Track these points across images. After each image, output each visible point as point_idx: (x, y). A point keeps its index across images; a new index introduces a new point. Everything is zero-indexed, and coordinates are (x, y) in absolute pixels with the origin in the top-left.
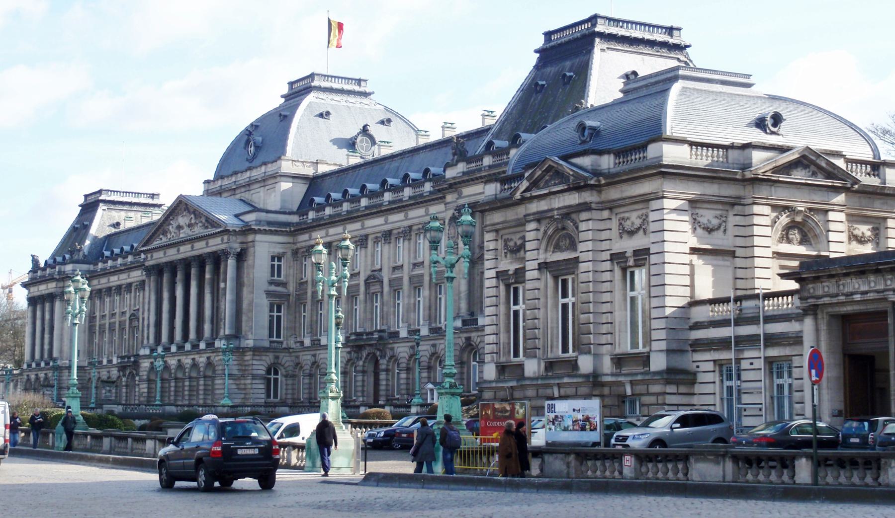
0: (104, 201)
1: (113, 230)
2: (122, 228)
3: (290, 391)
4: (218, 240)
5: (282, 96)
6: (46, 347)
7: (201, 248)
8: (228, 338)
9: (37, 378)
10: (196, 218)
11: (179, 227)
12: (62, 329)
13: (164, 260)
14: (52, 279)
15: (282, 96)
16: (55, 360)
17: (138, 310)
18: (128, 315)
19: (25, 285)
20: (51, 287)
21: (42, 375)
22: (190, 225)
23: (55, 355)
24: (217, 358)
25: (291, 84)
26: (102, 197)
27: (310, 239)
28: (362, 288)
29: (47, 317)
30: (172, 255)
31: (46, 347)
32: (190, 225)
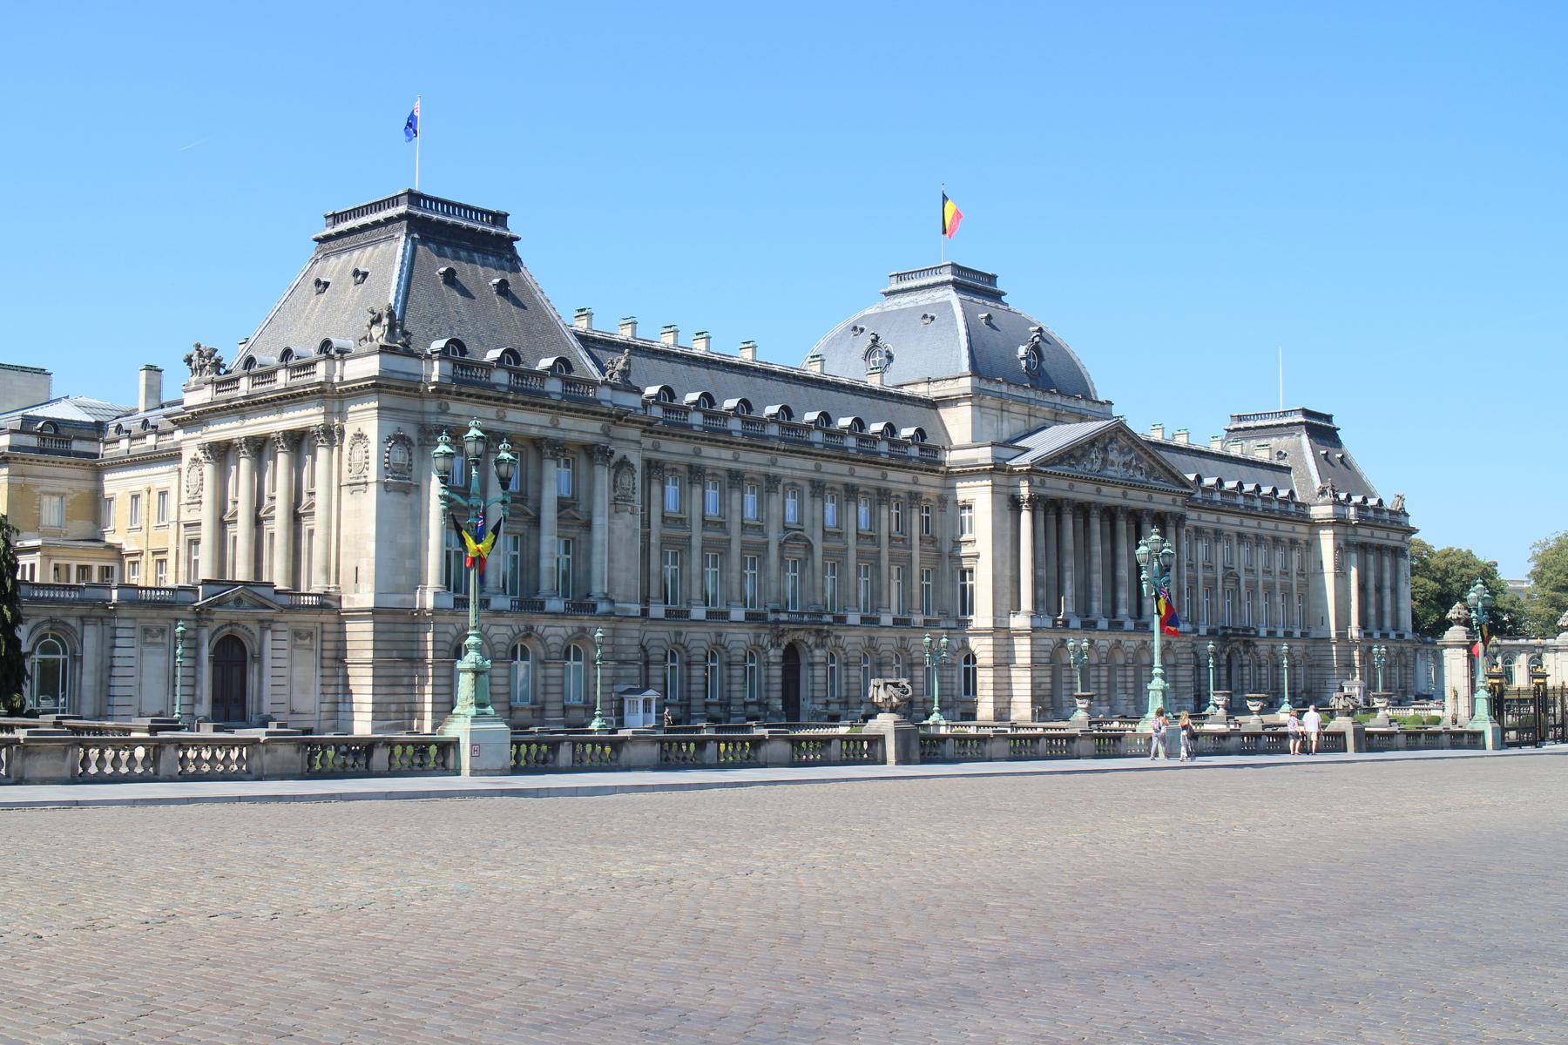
4: (1169, 499)
7: (1137, 499)
13: (1070, 495)
22: (1127, 465)
28: (1220, 583)
30: (1085, 492)
32: (1127, 465)
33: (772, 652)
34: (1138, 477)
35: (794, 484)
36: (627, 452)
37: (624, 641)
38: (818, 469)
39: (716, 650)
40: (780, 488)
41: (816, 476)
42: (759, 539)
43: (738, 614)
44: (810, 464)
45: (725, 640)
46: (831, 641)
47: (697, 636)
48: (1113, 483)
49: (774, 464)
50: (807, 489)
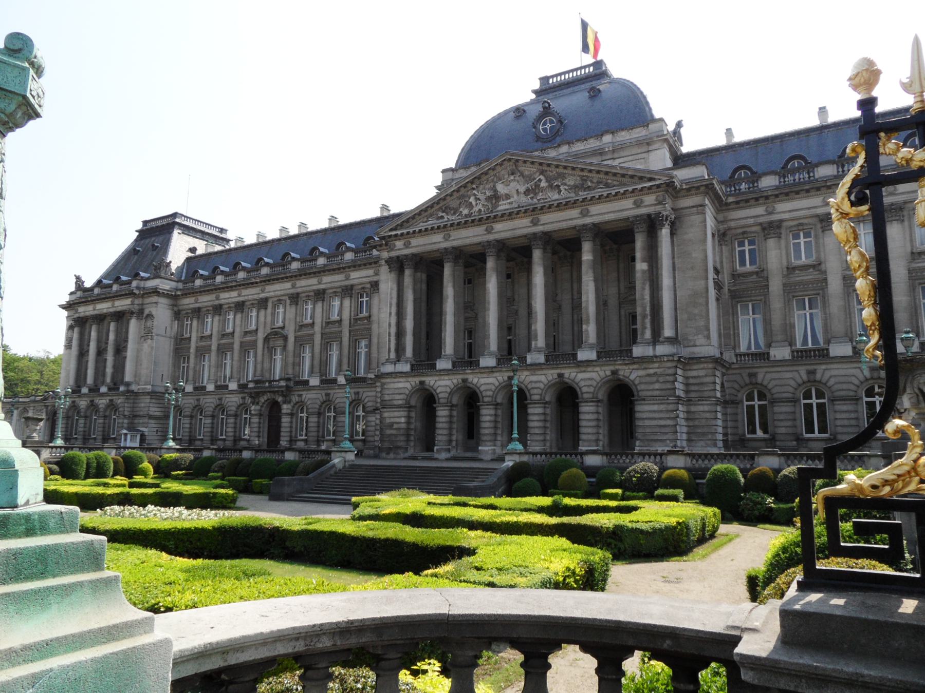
0: (180, 225)
1: (190, 254)
2: (199, 252)
3: (730, 424)
4: (628, 203)
5: (535, 92)
6: (109, 370)
8: (673, 341)
9: (92, 405)
10: (547, 181)
11: (495, 197)
12: (139, 351)
14: (131, 294)
15: (535, 92)
16: (128, 384)
17: (283, 328)
18: (261, 336)
19: (68, 307)
20: (122, 304)
21: (102, 402)
23: (128, 378)
24: (641, 373)
25: (544, 80)
26: (177, 220)
27: (771, 213)
29: (112, 337)
31: (109, 370)
33: (253, 408)
34: (556, 196)
35: (279, 300)
36: (151, 309)
37: (143, 405)
38: (293, 286)
39: (220, 407)
40: (270, 305)
41: (292, 291)
42: (254, 338)
43: (233, 386)
44: (288, 285)
45: (224, 401)
46: (295, 399)
47: (208, 400)
48: (510, 215)
49: (263, 291)
50: (288, 301)
